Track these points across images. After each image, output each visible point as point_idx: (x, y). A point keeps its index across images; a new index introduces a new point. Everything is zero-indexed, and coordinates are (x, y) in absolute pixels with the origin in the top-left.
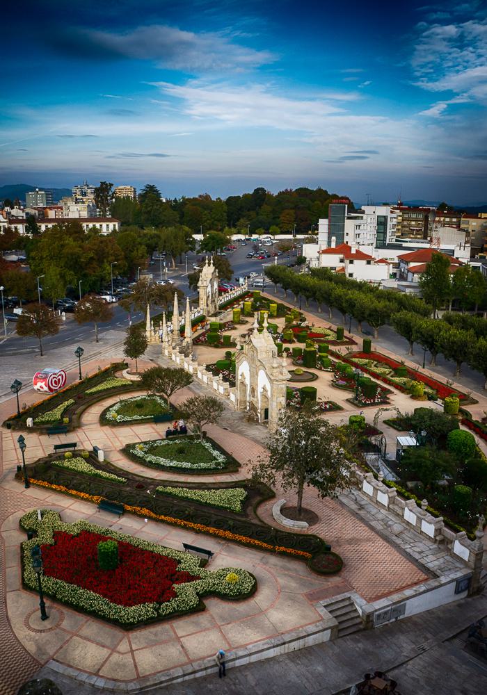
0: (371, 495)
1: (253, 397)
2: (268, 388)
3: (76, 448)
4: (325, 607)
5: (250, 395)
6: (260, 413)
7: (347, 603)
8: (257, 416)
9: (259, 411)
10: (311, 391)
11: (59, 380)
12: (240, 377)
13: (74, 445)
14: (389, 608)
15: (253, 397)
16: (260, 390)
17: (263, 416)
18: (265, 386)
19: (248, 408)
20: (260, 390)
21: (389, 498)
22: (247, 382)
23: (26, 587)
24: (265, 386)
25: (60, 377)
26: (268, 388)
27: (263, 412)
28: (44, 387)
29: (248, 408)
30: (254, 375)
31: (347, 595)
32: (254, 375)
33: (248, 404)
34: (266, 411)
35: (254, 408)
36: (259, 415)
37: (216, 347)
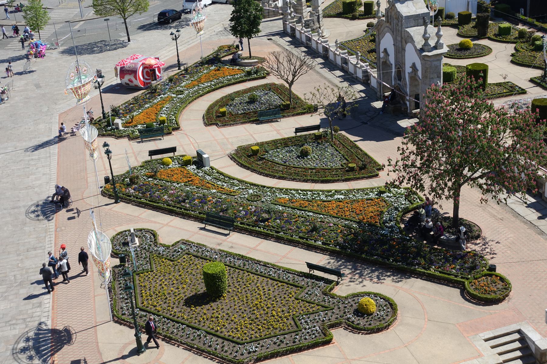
1: (400, 80)
2: (419, 66)
3: (176, 154)
4: (486, 340)
5: (395, 78)
6: (409, 101)
8: (406, 104)
10: (482, 68)
13: (173, 150)
15: (400, 80)
16: (408, 70)
20: (408, 70)
22: (392, 59)
23: (118, 320)
26: (419, 66)
28: (133, 79)
32: (400, 51)
34: (417, 97)
36: (408, 103)
37: (354, 18)
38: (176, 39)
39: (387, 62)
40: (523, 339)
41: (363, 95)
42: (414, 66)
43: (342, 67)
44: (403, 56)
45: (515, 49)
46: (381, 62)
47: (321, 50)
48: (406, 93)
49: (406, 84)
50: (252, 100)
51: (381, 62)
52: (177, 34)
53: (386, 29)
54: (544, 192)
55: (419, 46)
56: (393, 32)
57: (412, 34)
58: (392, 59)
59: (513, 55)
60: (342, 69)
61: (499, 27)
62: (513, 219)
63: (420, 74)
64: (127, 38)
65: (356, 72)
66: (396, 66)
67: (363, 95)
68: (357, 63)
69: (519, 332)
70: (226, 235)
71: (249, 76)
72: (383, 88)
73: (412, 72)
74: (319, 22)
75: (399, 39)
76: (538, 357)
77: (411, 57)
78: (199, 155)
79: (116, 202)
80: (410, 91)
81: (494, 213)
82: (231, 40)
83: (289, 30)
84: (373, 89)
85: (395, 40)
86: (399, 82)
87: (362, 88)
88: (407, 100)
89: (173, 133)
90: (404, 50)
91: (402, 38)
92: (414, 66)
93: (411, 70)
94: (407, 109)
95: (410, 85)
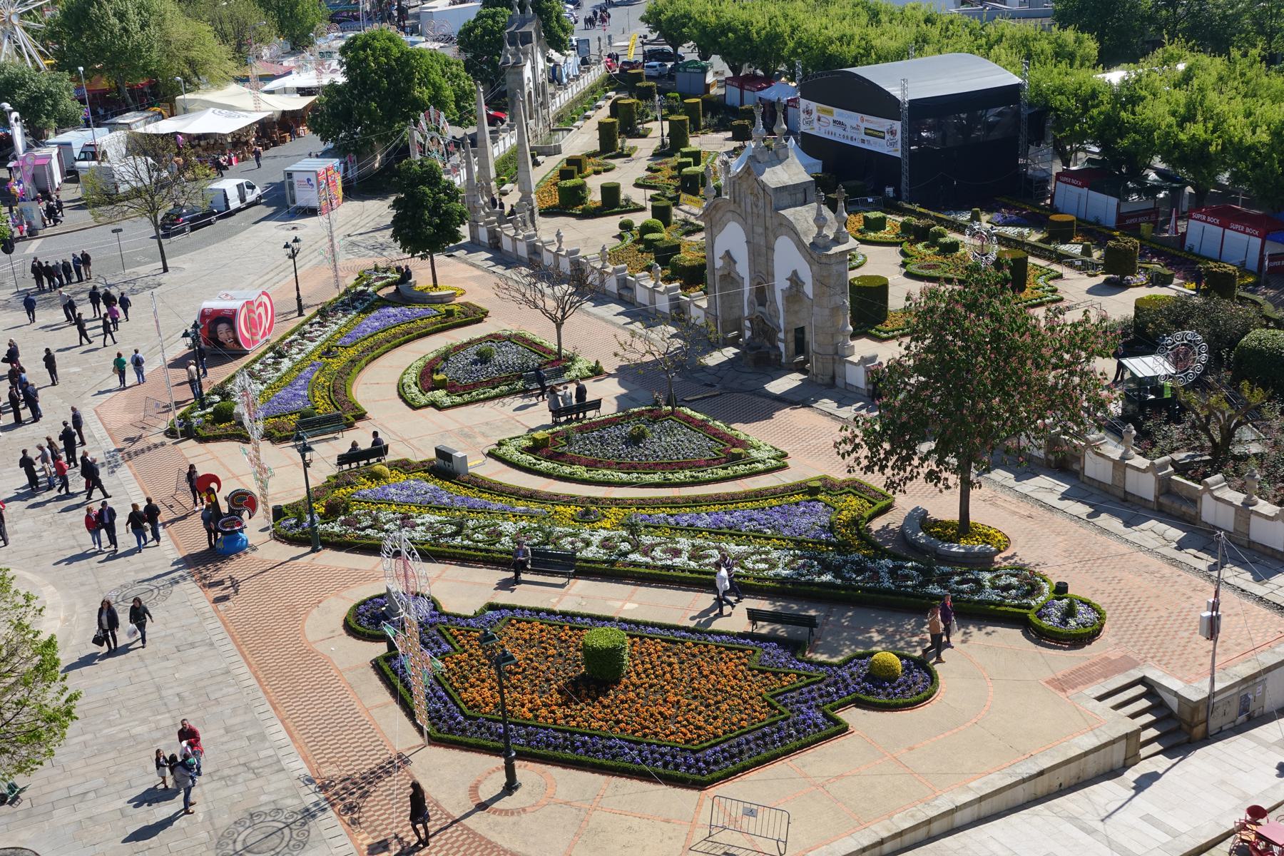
0: (1109, 480)
1: (762, 304)
5: (751, 303)
6: (785, 341)
7: (1140, 689)
9: (781, 335)
10: (877, 284)
11: (260, 315)
12: (719, 263)
14: (1235, 690)
15: (762, 304)
16: (781, 283)
17: (792, 346)
18: (795, 273)
19: (748, 334)
20: (781, 283)
22: (743, 268)
24: (795, 273)
25: (261, 310)
27: (791, 337)
29: (748, 334)
30: (761, 254)
31: (1136, 674)
32: (761, 254)
33: (747, 323)
34: (800, 332)
35: (764, 329)
36: (782, 346)
38: (293, 256)
39: (733, 274)
40: (1152, 690)
41: (678, 343)
42: (795, 280)
44: (769, 261)
45: (903, 253)
46: (717, 278)
47: (566, 266)
48: (779, 327)
50: (484, 358)
51: (717, 278)
52: (295, 245)
53: (729, 215)
54: (1083, 469)
55: (808, 240)
56: (745, 220)
57: (791, 219)
58: (743, 268)
59: (904, 265)
60: (620, 300)
61: (866, 218)
62: (1048, 515)
63: (809, 289)
64: (160, 264)
65: (653, 302)
66: (752, 280)
67: (678, 343)
68: (656, 285)
69: (1143, 681)
70: (562, 586)
71: (449, 322)
73: (791, 288)
74: (533, 222)
75: (760, 230)
76: (1187, 717)
77: (788, 260)
78: (443, 454)
79: (313, 551)
80: (786, 323)
81: (1013, 508)
82: (396, 255)
83: (483, 235)
84: (699, 330)
86: (761, 309)
87: (672, 330)
88: (780, 340)
89: (357, 424)
90: (770, 248)
91: (766, 228)
92: (795, 280)
93: (788, 284)
95: (787, 311)
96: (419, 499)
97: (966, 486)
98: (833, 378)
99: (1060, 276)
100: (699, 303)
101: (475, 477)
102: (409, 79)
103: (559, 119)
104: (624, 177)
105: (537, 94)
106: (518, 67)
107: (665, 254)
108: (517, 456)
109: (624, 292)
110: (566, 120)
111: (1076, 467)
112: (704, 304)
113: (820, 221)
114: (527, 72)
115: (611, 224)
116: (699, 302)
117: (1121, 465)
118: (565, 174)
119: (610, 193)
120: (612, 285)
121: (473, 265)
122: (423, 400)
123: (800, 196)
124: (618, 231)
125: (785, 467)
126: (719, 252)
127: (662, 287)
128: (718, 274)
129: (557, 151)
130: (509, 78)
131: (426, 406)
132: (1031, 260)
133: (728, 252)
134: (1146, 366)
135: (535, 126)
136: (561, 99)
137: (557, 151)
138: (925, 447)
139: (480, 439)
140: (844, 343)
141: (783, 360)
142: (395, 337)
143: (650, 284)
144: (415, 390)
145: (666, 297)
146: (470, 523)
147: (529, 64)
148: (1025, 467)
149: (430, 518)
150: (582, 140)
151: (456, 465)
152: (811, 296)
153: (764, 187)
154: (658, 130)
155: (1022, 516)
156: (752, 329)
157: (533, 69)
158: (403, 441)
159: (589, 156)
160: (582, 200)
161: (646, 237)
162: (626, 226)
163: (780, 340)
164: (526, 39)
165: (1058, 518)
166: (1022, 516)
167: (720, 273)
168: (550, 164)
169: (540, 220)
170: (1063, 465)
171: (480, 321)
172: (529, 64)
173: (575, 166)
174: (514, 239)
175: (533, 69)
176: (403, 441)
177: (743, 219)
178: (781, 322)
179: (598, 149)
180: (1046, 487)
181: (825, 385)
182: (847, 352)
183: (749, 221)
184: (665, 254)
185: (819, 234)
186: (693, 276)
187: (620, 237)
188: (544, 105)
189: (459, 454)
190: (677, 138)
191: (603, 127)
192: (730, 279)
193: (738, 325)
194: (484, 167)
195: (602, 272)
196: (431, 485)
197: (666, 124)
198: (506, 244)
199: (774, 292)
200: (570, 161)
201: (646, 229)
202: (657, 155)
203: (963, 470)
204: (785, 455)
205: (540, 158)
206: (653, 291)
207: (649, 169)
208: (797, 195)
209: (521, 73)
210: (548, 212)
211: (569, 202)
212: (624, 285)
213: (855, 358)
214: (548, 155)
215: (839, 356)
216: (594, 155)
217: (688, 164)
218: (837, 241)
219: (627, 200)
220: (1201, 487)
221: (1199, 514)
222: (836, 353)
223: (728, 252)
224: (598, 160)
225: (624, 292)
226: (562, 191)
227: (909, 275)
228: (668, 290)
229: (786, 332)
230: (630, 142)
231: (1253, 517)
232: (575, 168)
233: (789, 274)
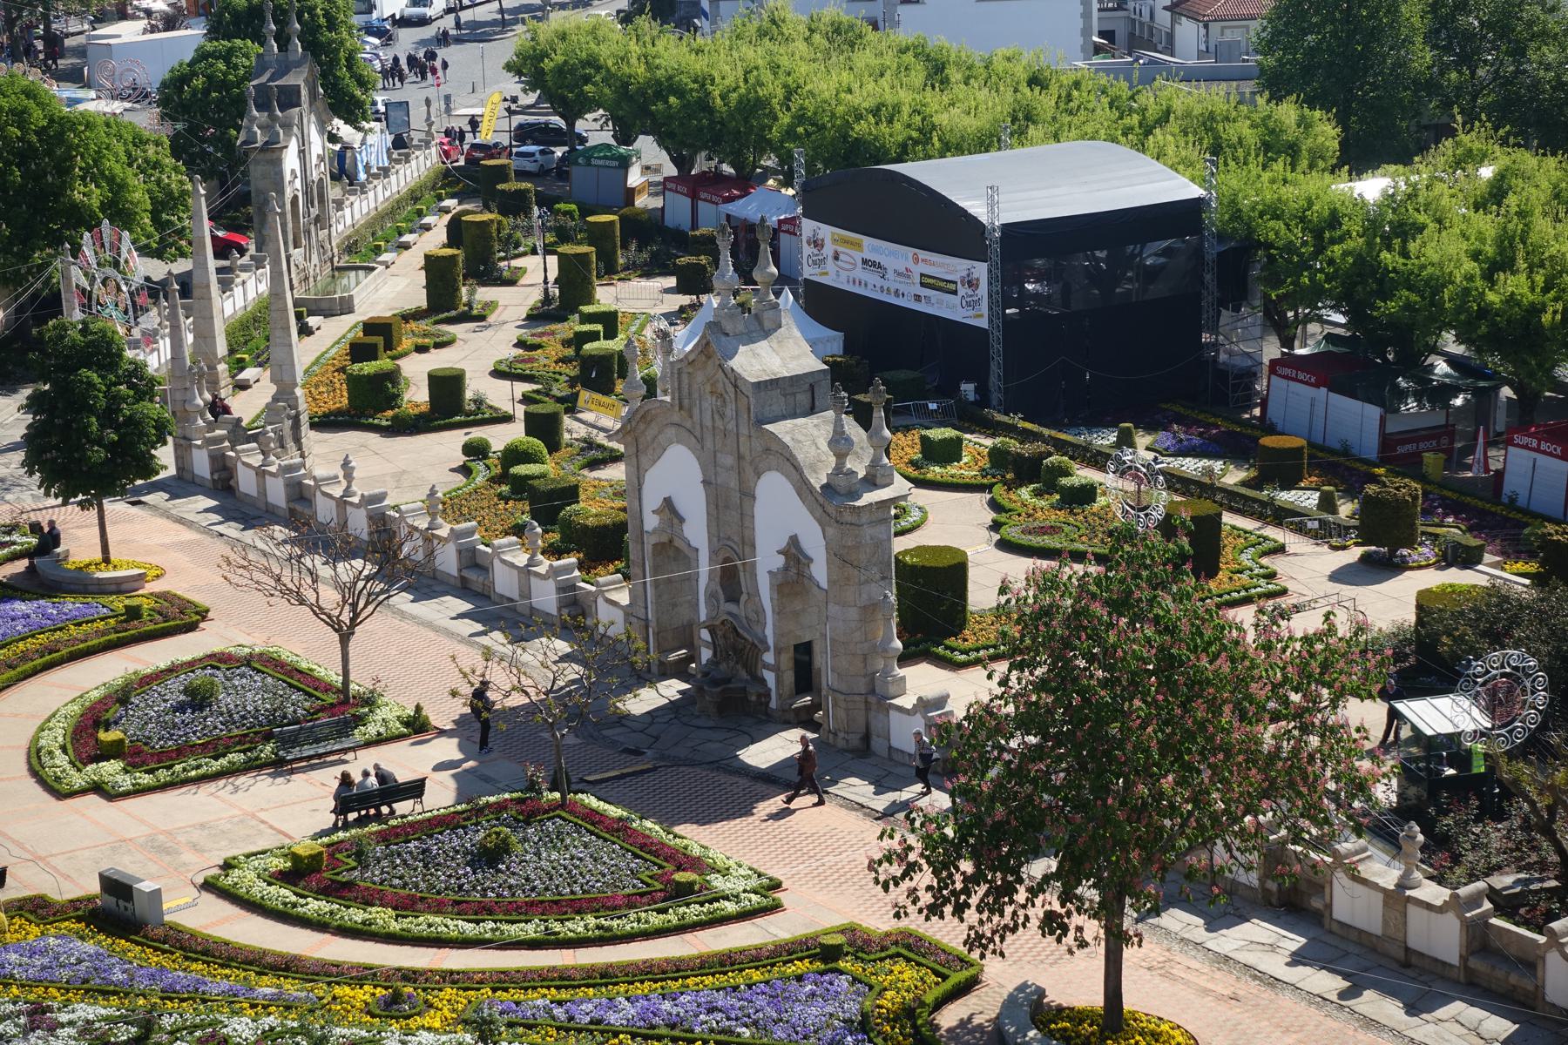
1: (733, 597)
2: (815, 543)
5: (711, 596)
6: (775, 668)
8: (763, 681)
9: (769, 658)
12: (651, 522)
16: (767, 559)
17: (789, 677)
18: (794, 541)
19: (706, 654)
20: (767, 559)
21: (1464, 921)
22: (696, 531)
24: (794, 541)
26: (815, 543)
27: (787, 660)
30: (731, 507)
32: (731, 507)
33: (705, 634)
35: (737, 646)
36: (770, 677)
39: (678, 542)
41: (573, 671)
42: (794, 553)
43: (463, 579)
45: (994, 505)
46: (648, 549)
47: (359, 524)
48: (764, 641)
49: (760, 611)
50: (198, 700)
51: (648, 549)
53: (671, 431)
54: (1329, 906)
55: (818, 480)
56: (701, 440)
57: (787, 439)
58: (696, 531)
59: (996, 526)
60: (462, 589)
61: (924, 439)
62: (1267, 994)
63: (820, 571)
65: (526, 593)
66: (713, 552)
67: (573, 671)
68: (532, 562)
71: (133, 628)
72: (657, 634)
73: (786, 568)
74: (297, 440)
75: (728, 460)
77: (779, 517)
81: (1203, 982)
82: (31, 500)
83: (201, 464)
84: (611, 645)
85: (710, 467)
86: (731, 607)
87: (562, 646)
88: (767, 667)
90: (748, 495)
91: (740, 457)
92: (794, 553)
94: (768, 694)
95: (779, 612)
96: (65, 974)
97: (1116, 941)
98: (867, 738)
99: (1280, 549)
100: (614, 596)
101: (173, 927)
102: (63, 169)
103: (350, 248)
104: (478, 353)
105: (309, 202)
106: (272, 151)
107: (550, 504)
108: (260, 890)
109: (472, 575)
110: (363, 251)
111: (1316, 903)
112: (623, 598)
113: (840, 445)
114: (290, 161)
115: (447, 446)
116: (614, 595)
117: (1397, 899)
118: (359, 352)
119: (447, 387)
120: (448, 560)
121: (180, 521)
122: (78, 780)
123: (803, 399)
124: (460, 459)
125: (775, 908)
126: (651, 500)
127: (544, 565)
128: (650, 541)
129: (346, 307)
130: (256, 172)
131: (83, 792)
132: (1228, 518)
133: (668, 502)
134: (1441, 714)
135: (305, 265)
136: (355, 212)
137: (346, 307)
138: (1039, 868)
139: (188, 856)
140: (887, 672)
141: (773, 704)
142: (25, 657)
143: (521, 559)
144: (61, 760)
145: (551, 585)
146: (166, 1021)
147: (293, 146)
148: (1222, 905)
149: (86, 1011)
150: (393, 287)
151: (140, 907)
152: (824, 584)
153: (735, 380)
154: (537, 272)
155: (1220, 998)
156: (714, 645)
157: (302, 153)
158: (36, 859)
159: (407, 317)
160: (392, 400)
161: (513, 470)
162: (476, 451)
163: (767, 667)
164: (289, 98)
165: (1286, 1000)
166: (1220, 998)
167: (653, 540)
168: (332, 333)
169: (310, 437)
170: (1294, 900)
171: (191, 627)
172: (293, 146)
173: (379, 336)
174: (261, 473)
175: (302, 153)
176: (36, 859)
177: (697, 440)
178: (769, 632)
179: (424, 304)
180: (1262, 942)
181: (849, 749)
182: (892, 690)
183: (709, 444)
184: (550, 504)
185: (839, 469)
186: (603, 545)
187: (465, 470)
188: (321, 221)
189: (146, 886)
190: (572, 290)
191: (433, 266)
192: (672, 551)
193: (686, 637)
194: (204, 335)
195: (429, 538)
196: (89, 947)
197: (553, 261)
198: (246, 482)
199: (754, 575)
200: (371, 327)
201: (514, 455)
202: (536, 317)
203: (1109, 912)
204: (776, 886)
205: (312, 321)
206: (526, 572)
207: (520, 344)
208: (796, 395)
209: (278, 163)
210: (327, 423)
211: (368, 403)
212: (472, 561)
213: (907, 701)
214: (328, 314)
215: (877, 696)
216: (416, 315)
217: (594, 336)
218: (871, 482)
219: (479, 402)
220: (1542, 939)
221: (1540, 989)
222: (873, 692)
223: (668, 502)
224: (424, 325)
225: (472, 575)
226: (355, 383)
227: (1005, 545)
228: (553, 572)
229: (778, 652)
230: (485, 294)
231: (1412, 910)
232: (380, 340)
233: (783, 544)
